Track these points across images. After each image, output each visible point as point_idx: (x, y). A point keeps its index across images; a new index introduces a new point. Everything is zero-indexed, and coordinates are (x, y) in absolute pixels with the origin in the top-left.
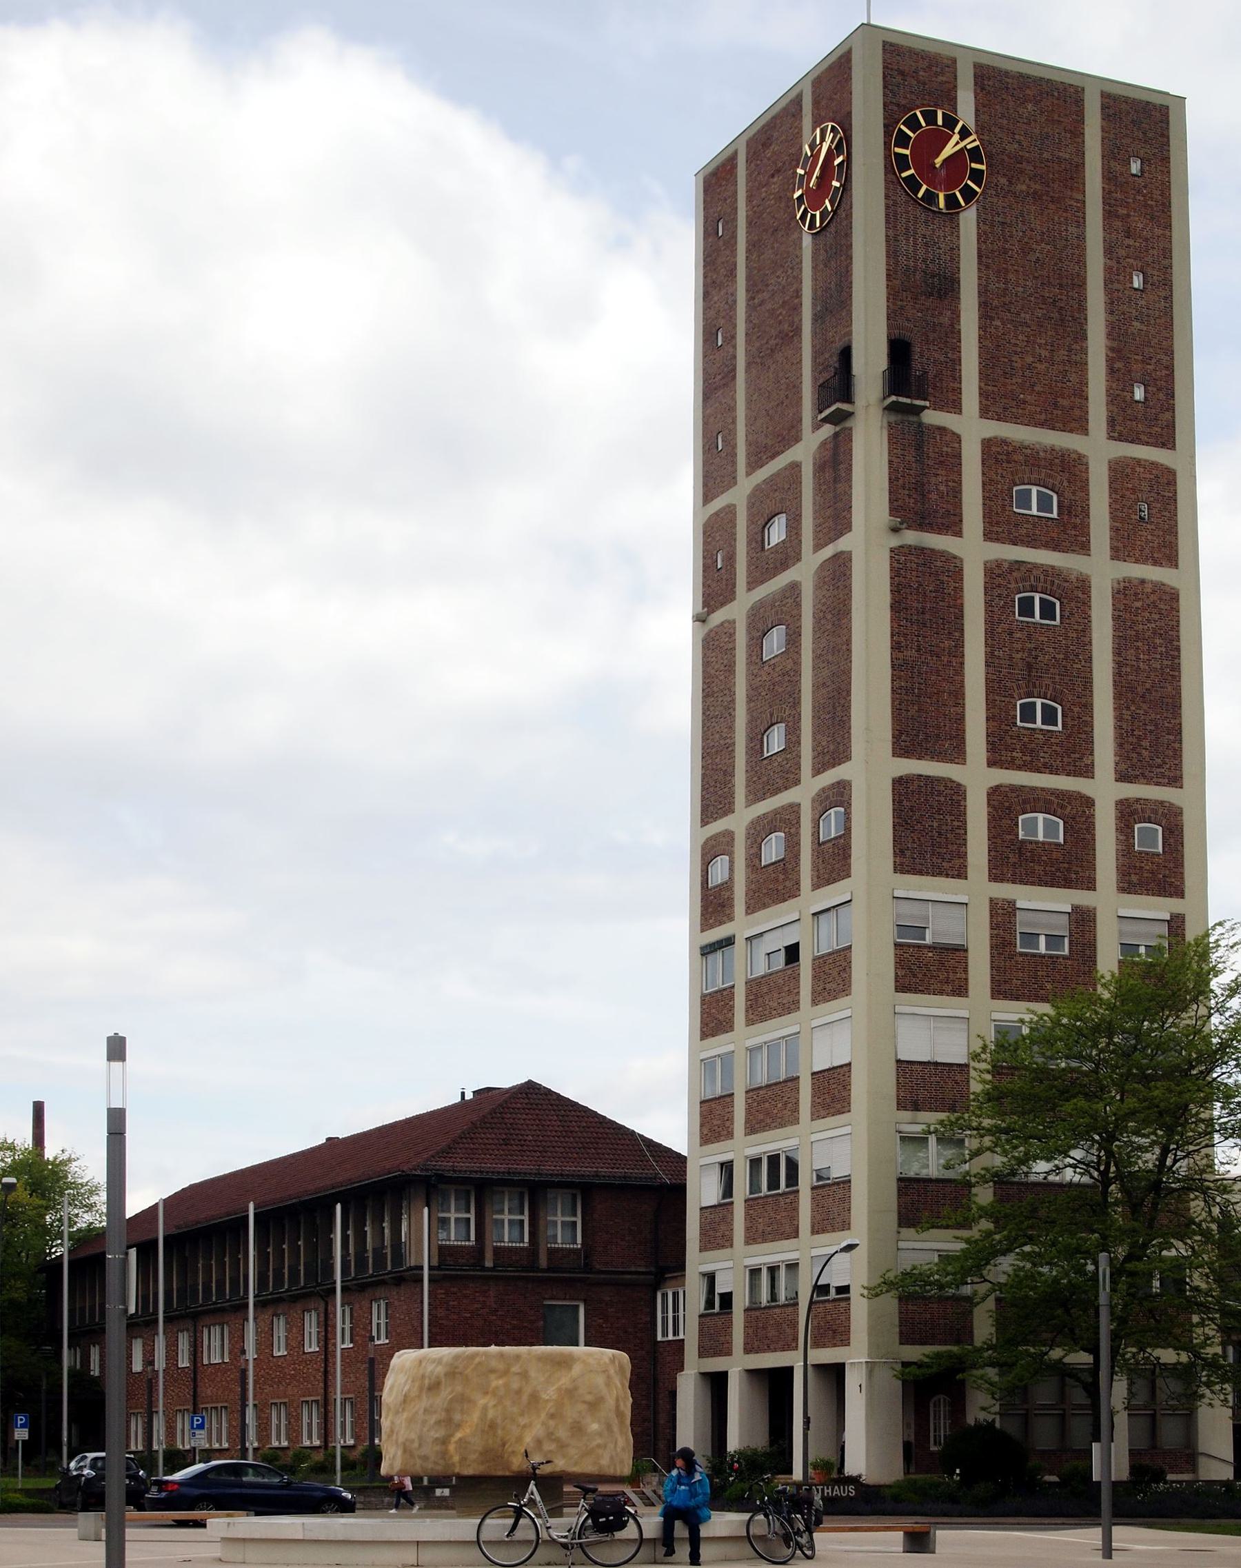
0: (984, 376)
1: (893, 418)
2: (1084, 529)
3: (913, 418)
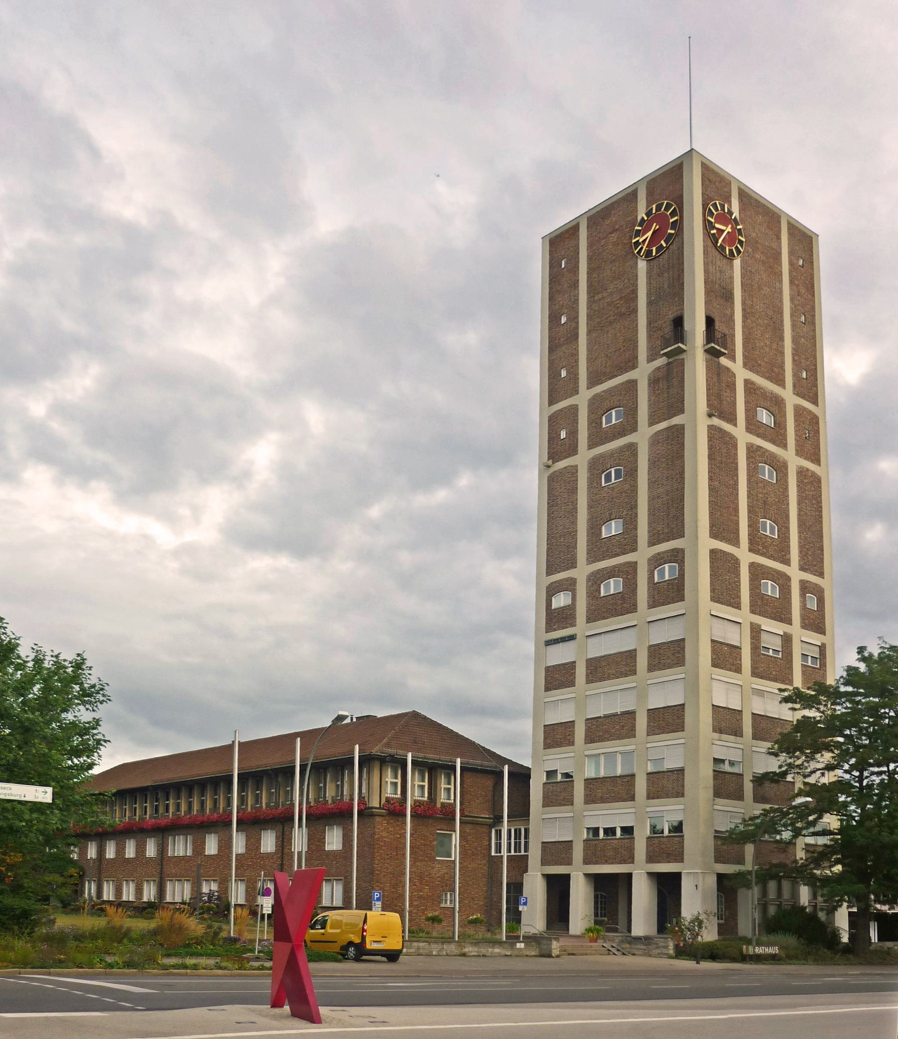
1: (709, 357)
2: (784, 436)
3: (716, 359)
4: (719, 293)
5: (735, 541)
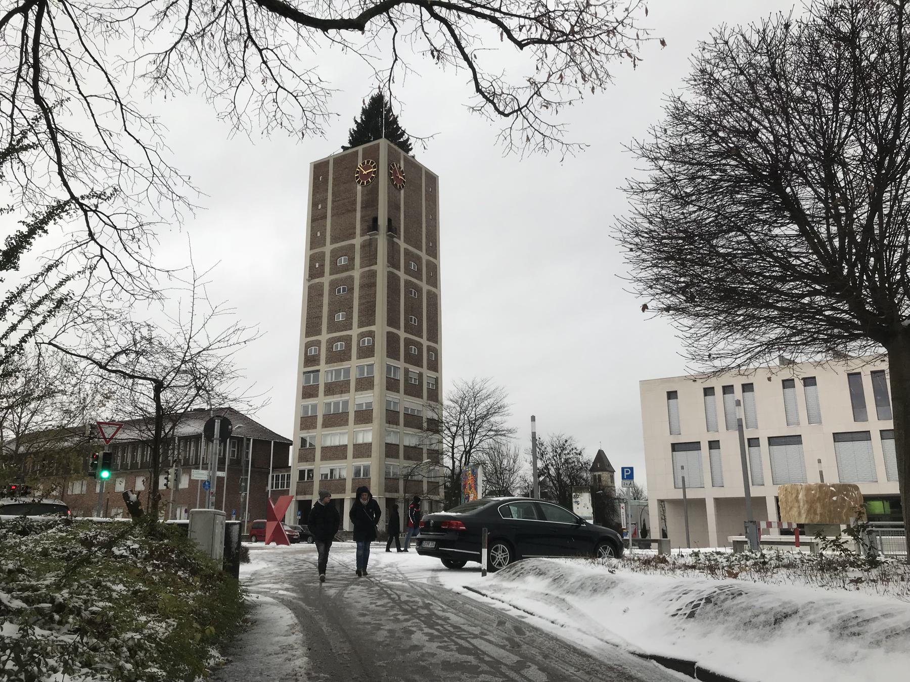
0: (405, 232)
4: (393, 206)
5: (398, 328)
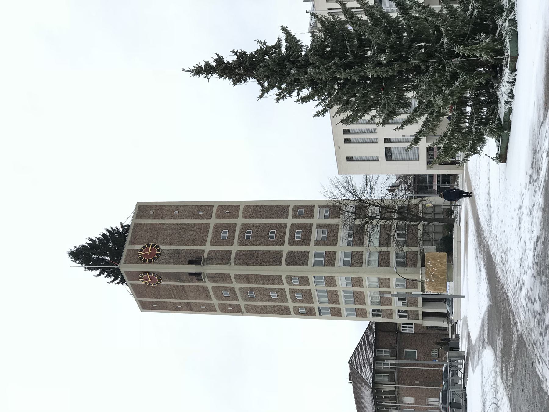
1: (205, 264)
2: (231, 225)
